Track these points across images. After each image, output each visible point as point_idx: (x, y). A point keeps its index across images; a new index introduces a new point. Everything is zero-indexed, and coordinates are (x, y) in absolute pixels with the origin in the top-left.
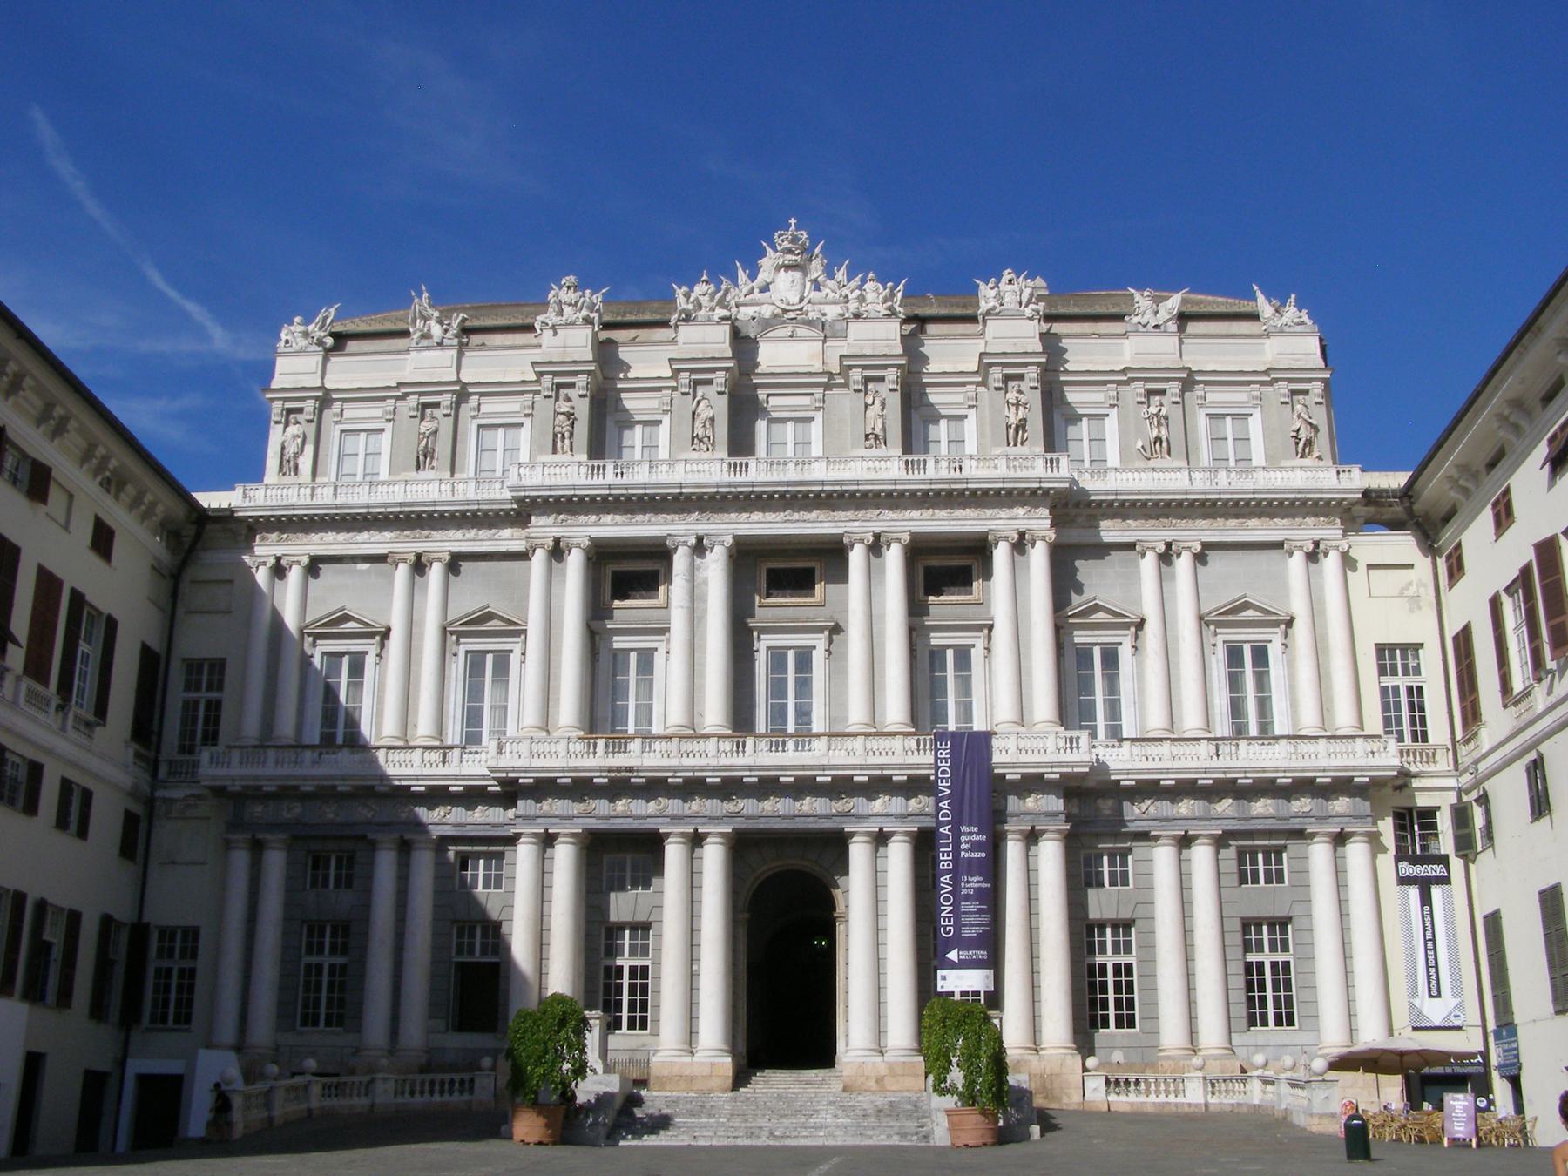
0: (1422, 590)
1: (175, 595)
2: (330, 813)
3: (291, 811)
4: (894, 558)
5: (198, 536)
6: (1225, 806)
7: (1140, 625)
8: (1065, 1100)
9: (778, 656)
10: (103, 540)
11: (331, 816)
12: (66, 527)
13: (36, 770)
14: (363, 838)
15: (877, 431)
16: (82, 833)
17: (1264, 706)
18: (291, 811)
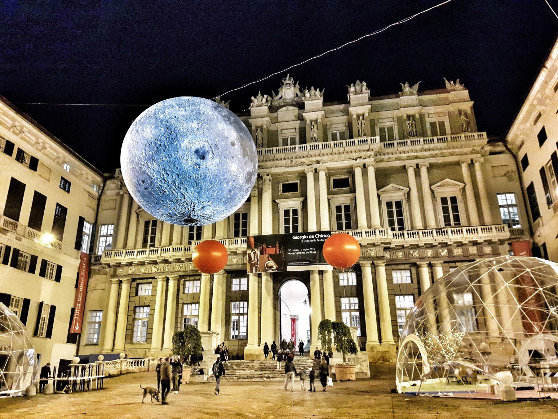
0: (513, 174)
1: (98, 205)
2: (143, 270)
3: (131, 270)
4: (322, 176)
5: (104, 186)
6: (444, 253)
7: (409, 194)
8: (391, 361)
9: (287, 212)
10: (66, 185)
11: (143, 271)
12: (49, 181)
13: (34, 259)
14: (154, 278)
15: (315, 135)
16: (58, 279)
17: (457, 218)
18: (131, 270)
